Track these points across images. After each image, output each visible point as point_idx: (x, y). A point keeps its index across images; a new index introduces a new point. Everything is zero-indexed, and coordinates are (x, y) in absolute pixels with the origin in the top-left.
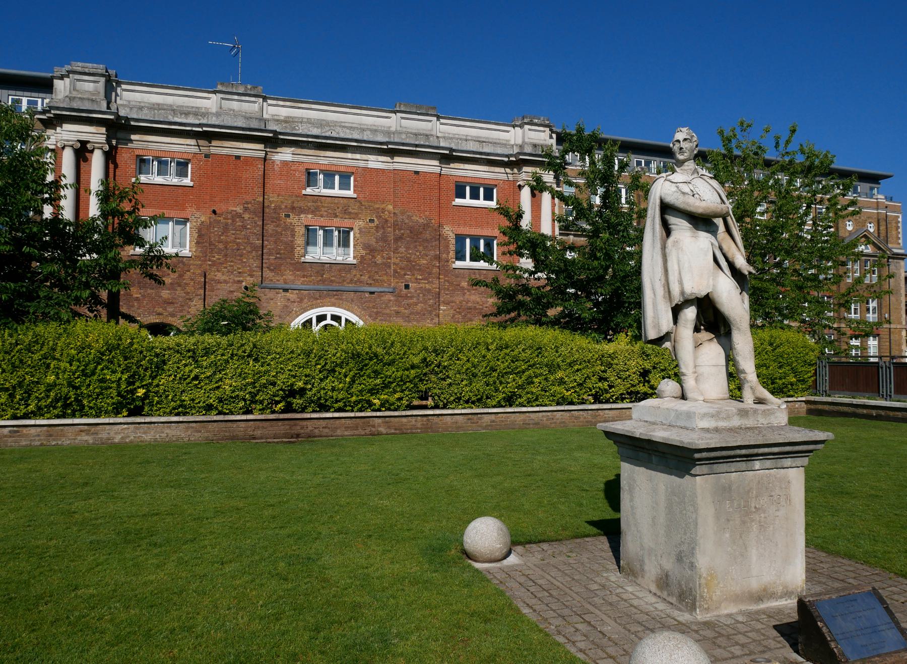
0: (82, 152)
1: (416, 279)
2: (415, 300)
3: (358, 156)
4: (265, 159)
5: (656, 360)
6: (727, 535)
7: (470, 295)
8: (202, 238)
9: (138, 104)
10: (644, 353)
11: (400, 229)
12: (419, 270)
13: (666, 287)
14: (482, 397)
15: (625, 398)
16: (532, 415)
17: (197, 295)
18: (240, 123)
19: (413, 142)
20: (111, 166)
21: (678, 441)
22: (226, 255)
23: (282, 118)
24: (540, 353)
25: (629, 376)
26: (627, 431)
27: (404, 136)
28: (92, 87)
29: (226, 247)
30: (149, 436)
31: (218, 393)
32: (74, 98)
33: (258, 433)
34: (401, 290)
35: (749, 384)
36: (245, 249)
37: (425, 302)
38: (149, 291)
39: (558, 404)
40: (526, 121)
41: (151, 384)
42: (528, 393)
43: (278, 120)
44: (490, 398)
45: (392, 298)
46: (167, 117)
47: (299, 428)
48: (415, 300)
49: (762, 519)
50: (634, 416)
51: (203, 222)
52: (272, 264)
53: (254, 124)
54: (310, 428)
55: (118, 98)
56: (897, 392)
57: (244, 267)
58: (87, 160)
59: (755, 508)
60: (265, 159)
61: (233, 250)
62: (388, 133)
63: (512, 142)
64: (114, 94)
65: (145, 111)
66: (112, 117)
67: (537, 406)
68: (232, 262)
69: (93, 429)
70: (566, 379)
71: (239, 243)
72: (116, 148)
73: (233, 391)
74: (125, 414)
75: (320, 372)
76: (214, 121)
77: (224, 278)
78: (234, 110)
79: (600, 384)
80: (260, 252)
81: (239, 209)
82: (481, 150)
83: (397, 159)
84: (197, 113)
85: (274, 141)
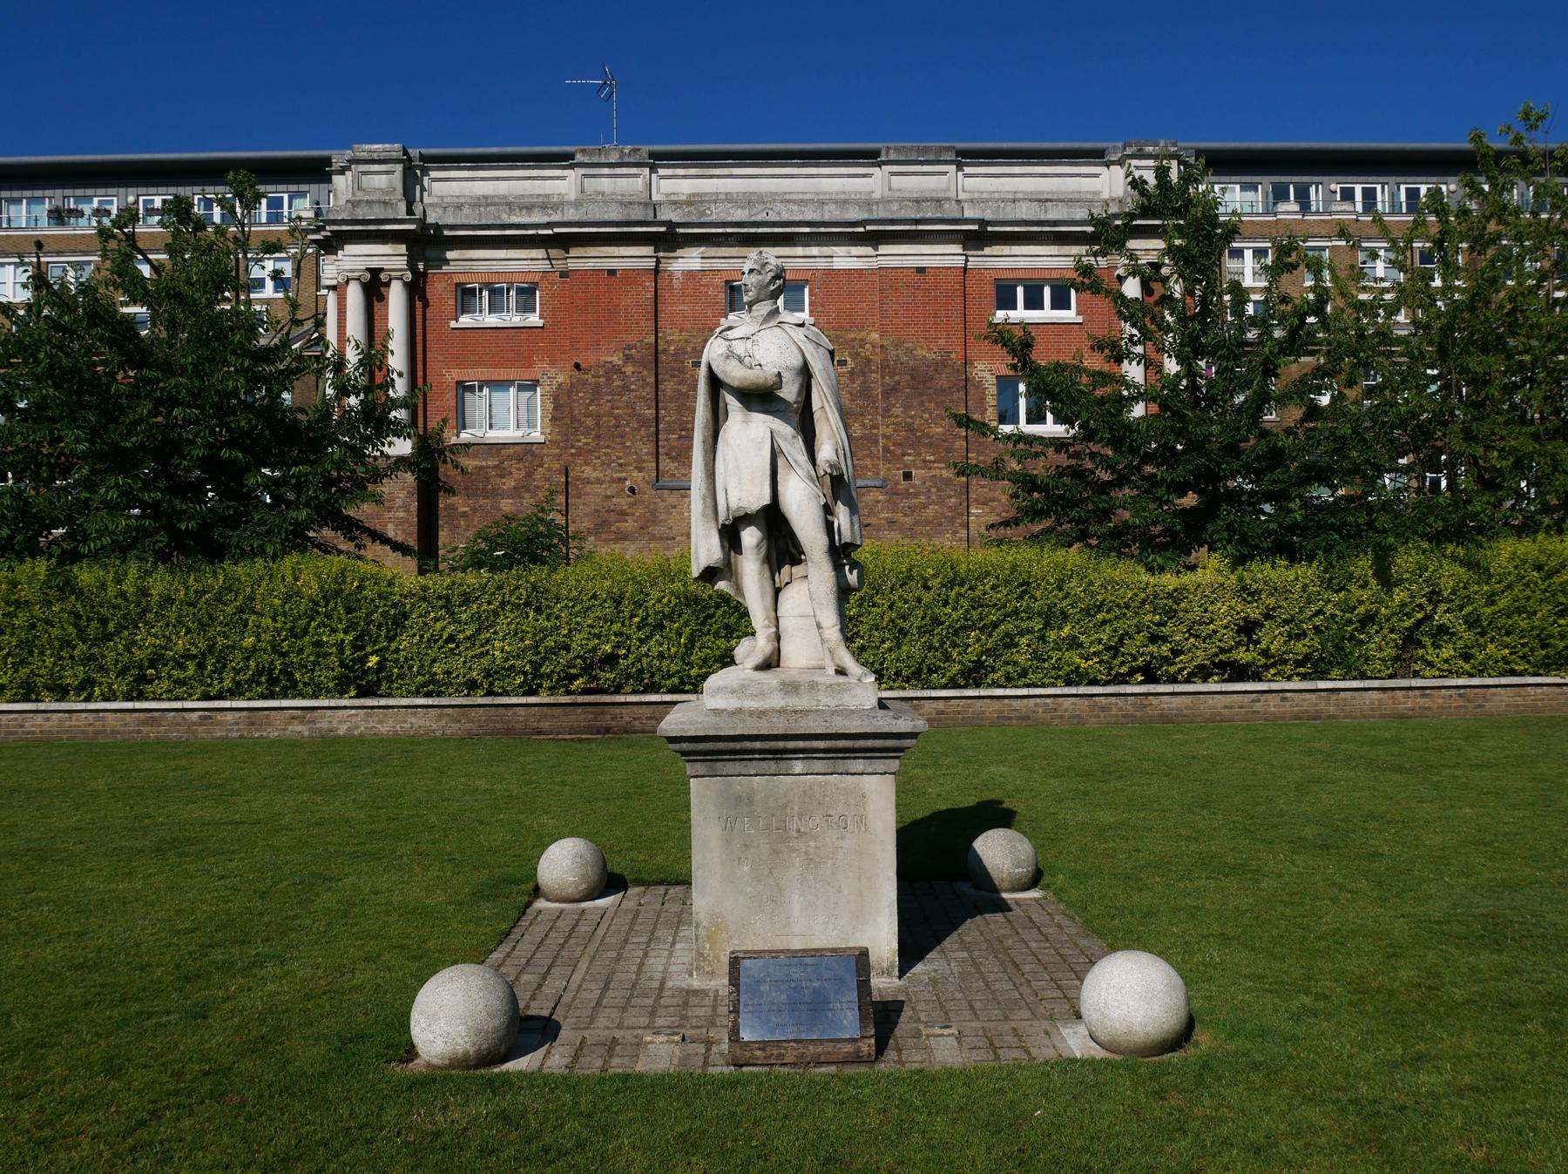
0: (374, 287)
1: (925, 461)
2: (922, 499)
3: (815, 251)
4: (656, 271)
5: (1271, 601)
6: (746, 869)
8: (561, 412)
9: (455, 200)
10: (1244, 589)
11: (892, 375)
12: (930, 445)
13: (709, 501)
14: (919, 670)
15: (1211, 675)
16: (1015, 703)
18: (614, 214)
19: (912, 216)
20: (419, 305)
22: (598, 437)
23: (683, 198)
24: (1025, 592)
25: (1215, 632)
27: (895, 207)
28: (385, 181)
29: (597, 424)
30: (386, 726)
31: (485, 661)
32: (359, 202)
33: (545, 725)
34: (897, 483)
37: (941, 502)
38: (482, 501)
39: (1069, 683)
40: (1129, 151)
41: (387, 648)
42: (1007, 663)
43: (675, 203)
44: (936, 672)
45: (881, 498)
46: (499, 217)
47: (608, 717)
48: (922, 499)
49: (812, 850)
51: (560, 385)
52: (673, 447)
53: (637, 214)
54: (626, 719)
55: (425, 194)
57: (627, 455)
58: (383, 298)
59: (798, 831)
60: (656, 271)
61: (609, 427)
62: (868, 204)
63: (1106, 195)
64: (418, 187)
65: (466, 210)
66: (413, 227)
67: (1028, 686)
68: (608, 447)
69: (309, 715)
70: (1082, 638)
71: (619, 415)
72: (425, 274)
73: (507, 660)
74: (352, 693)
75: (639, 628)
76: (571, 215)
77: (595, 474)
78: (603, 194)
79: (1153, 648)
80: (653, 429)
81: (616, 359)
82: (1043, 217)
83: (884, 249)
84: (545, 204)
85: (669, 239)
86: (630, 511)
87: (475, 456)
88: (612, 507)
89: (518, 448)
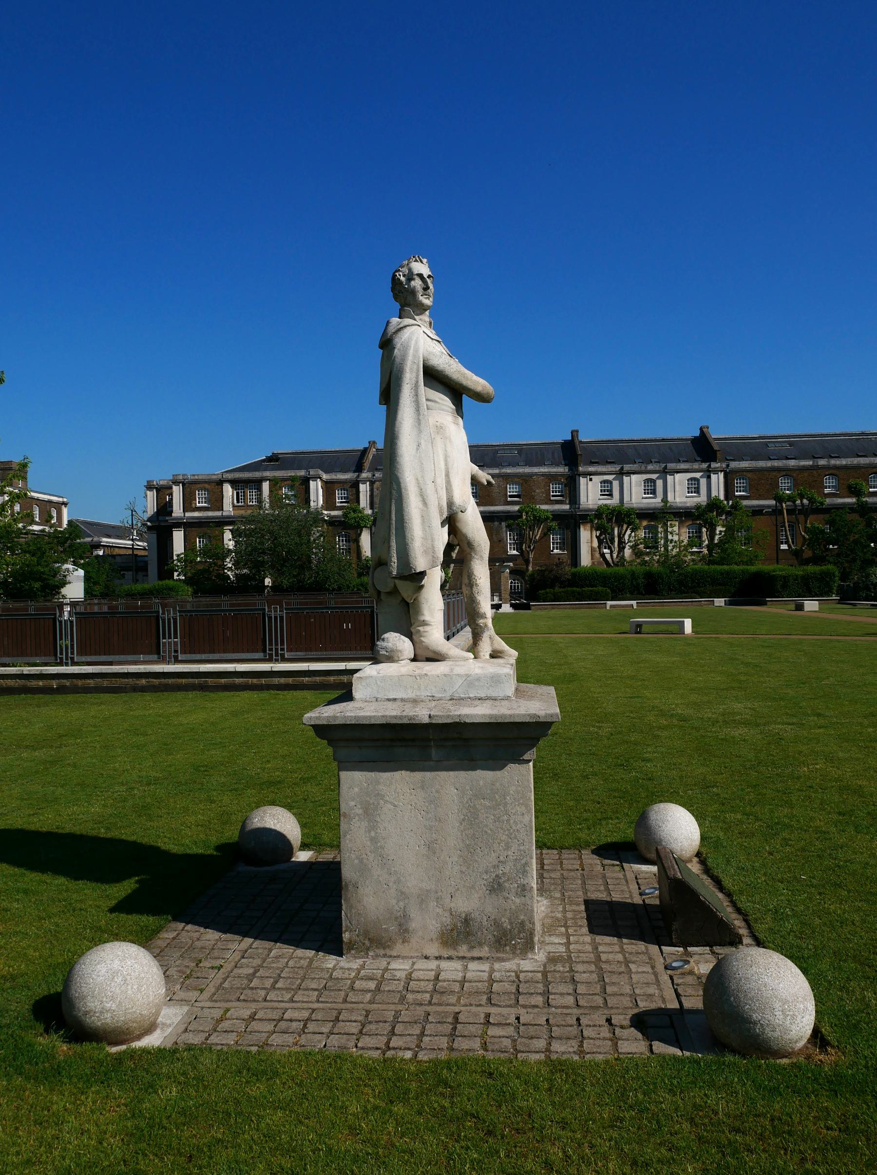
21: (524, 715)
26: (395, 717)
35: (489, 633)
50: (357, 693)
56: (80, 653)
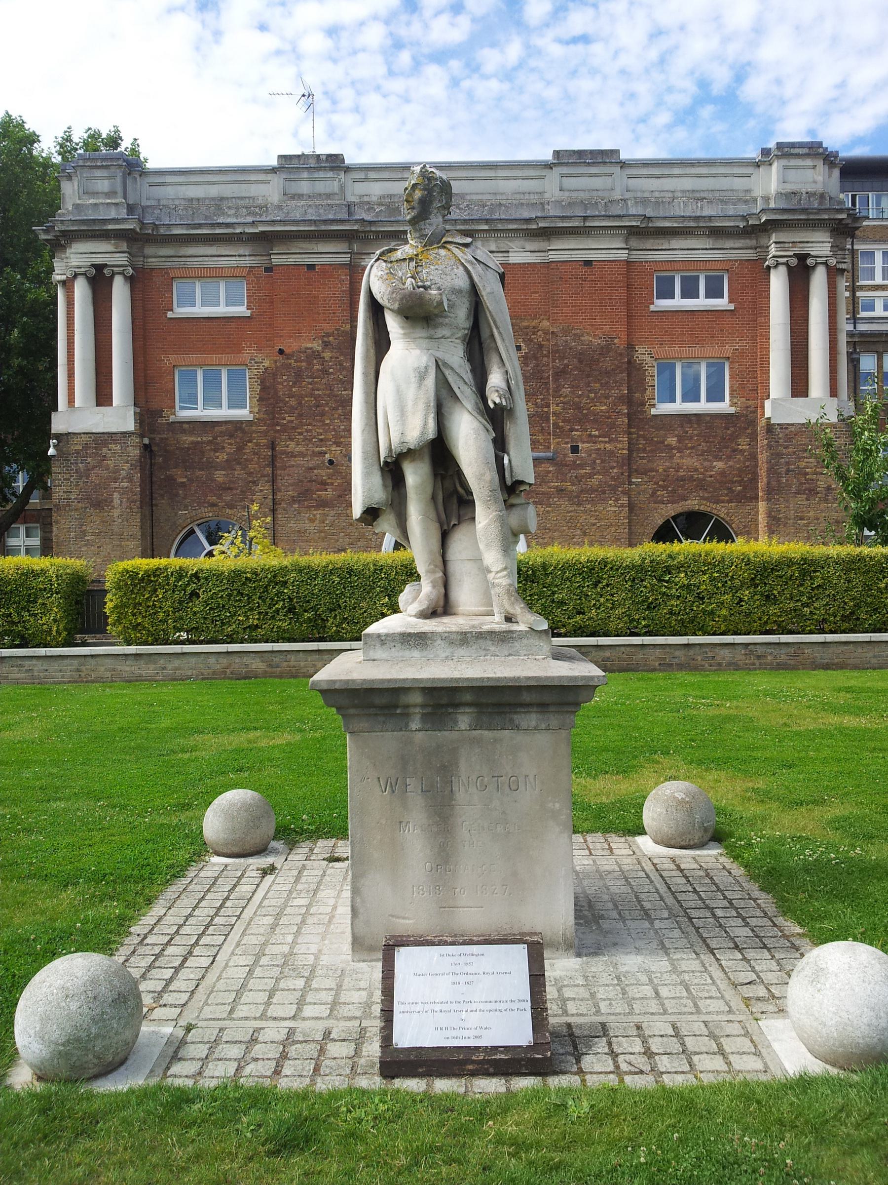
1: (590, 436)
2: (588, 470)
7: (682, 457)
11: (562, 358)
12: (596, 421)
17: (263, 476)
22: (300, 415)
29: (300, 403)
34: (565, 455)
36: (327, 404)
37: (605, 472)
38: (199, 473)
45: (551, 469)
48: (588, 470)
51: (266, 369)
61: (310, 407)
77: (299, 449)
81: (316, 346)
86: (329, 481)
87: (191, 432)
88: (314, 478)
89: (230, 426)
